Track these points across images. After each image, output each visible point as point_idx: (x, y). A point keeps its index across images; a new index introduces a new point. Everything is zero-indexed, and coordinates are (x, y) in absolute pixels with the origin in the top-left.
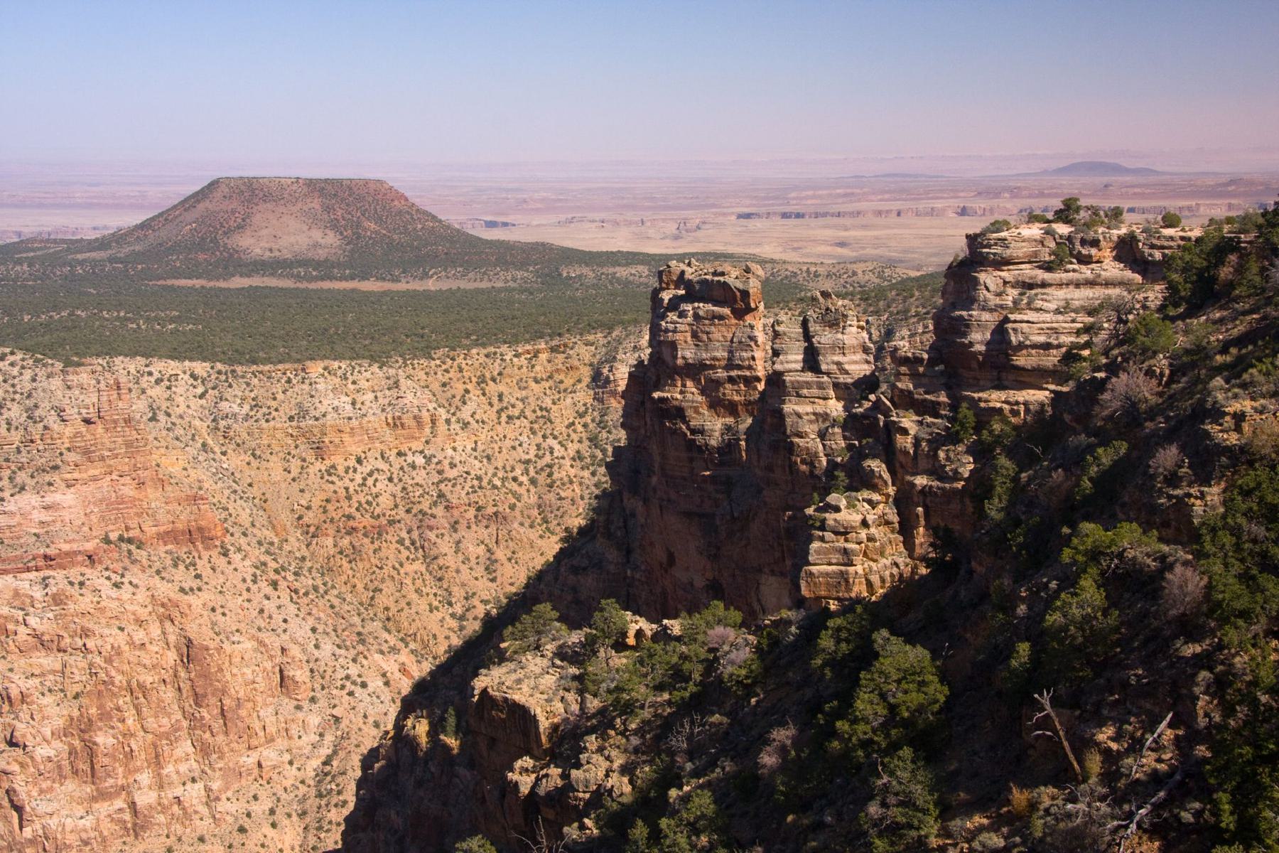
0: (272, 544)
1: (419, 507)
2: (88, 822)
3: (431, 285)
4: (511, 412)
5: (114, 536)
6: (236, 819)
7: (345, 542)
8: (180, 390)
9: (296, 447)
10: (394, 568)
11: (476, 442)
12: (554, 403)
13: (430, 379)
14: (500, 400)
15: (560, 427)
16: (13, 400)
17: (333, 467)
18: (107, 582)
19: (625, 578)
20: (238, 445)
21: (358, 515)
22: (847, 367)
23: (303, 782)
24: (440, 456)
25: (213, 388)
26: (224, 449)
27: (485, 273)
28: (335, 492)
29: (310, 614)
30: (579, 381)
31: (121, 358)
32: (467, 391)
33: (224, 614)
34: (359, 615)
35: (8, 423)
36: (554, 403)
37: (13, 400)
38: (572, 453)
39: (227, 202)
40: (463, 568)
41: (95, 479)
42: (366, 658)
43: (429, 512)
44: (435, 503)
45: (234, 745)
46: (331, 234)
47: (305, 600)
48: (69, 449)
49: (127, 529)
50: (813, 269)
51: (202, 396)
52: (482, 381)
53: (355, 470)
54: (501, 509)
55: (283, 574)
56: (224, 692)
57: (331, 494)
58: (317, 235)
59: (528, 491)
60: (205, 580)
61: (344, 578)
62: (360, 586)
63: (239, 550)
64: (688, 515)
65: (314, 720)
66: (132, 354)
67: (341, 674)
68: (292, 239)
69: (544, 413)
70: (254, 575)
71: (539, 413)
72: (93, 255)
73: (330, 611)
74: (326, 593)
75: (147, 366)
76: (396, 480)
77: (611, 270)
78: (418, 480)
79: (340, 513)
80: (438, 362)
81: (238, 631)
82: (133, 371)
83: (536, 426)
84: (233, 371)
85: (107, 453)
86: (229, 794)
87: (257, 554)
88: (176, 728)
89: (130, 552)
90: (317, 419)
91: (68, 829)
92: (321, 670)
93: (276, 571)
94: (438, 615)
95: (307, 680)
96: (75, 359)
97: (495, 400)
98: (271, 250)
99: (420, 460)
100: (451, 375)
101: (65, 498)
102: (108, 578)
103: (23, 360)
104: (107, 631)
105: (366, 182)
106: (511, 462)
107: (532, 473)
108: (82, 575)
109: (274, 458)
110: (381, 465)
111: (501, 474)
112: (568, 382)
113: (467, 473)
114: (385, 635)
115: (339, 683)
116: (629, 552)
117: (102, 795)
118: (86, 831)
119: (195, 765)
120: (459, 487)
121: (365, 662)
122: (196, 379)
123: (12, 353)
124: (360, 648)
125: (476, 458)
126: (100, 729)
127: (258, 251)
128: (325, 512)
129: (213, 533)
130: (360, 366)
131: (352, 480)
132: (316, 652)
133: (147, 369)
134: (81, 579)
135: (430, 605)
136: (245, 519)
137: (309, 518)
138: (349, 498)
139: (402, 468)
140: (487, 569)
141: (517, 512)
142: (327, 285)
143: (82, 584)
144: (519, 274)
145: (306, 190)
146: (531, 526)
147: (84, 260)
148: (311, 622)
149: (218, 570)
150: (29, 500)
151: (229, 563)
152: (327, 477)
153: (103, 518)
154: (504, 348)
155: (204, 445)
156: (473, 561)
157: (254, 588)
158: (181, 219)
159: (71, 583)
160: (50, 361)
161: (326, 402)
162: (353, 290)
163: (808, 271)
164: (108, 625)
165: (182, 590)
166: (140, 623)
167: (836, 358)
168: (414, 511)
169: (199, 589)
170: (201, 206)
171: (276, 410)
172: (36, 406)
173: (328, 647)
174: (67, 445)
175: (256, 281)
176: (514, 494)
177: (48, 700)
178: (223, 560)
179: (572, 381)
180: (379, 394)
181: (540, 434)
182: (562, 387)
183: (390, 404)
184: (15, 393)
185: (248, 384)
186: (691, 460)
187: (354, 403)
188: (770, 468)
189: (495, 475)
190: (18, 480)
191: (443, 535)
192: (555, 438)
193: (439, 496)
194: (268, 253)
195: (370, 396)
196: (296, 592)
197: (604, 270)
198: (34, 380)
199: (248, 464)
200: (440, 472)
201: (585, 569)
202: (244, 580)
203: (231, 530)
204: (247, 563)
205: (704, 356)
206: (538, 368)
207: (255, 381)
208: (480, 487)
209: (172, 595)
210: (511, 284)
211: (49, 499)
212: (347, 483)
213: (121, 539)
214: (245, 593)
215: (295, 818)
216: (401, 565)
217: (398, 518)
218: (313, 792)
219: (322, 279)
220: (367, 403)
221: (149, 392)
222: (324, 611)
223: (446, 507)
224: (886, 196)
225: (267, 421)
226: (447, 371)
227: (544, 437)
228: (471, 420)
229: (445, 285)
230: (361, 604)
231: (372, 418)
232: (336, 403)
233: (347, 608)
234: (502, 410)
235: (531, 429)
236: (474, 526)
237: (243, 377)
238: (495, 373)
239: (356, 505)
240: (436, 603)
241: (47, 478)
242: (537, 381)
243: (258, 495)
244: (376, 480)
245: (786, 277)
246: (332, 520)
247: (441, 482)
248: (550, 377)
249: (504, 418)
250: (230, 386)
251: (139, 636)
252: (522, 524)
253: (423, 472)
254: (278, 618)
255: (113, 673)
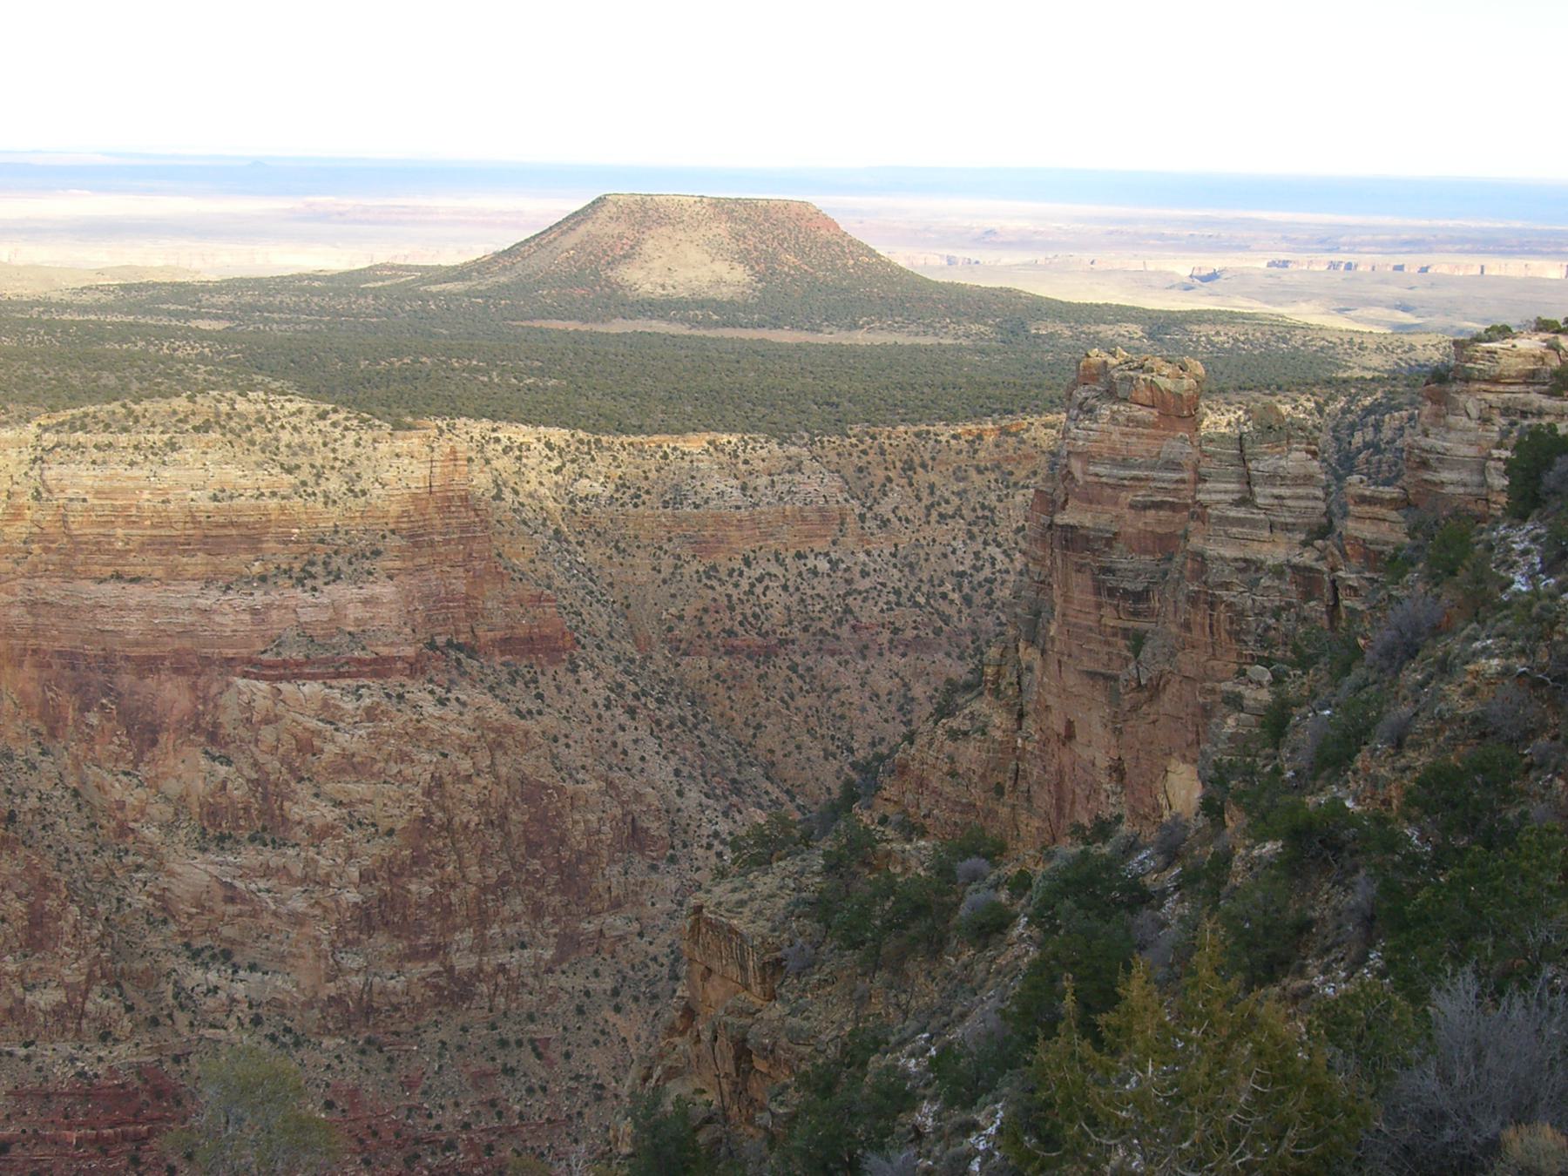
0: (632, 661)
1: (820, 625)
2: (398, 984)
3: (861, 338)
4: (944, 508)
5: (441, 640)
6: (572, 997)
7: (721, 664)
8: (531, 462)
9: (670, 540)
10: (782, 700)
11: (896, 546)
12: (1000, 500)
13: (843, 461)
14: (932, 493)
15: (1005, 533)
16: (333, 468)
17: (714, 568)
18: (430, 697)
19: (1015, 749)
20: (599, 534)
21: (740, 630)
22: (1289, 502)
23: (655, 959)
24: (849, 562)
25: (573, 461)
26: (581, 538)
27: (929, 325)
28: (715, 600)
29: (673, 752)
30: (1035, 473)
31: (464, 419)
32: (890, 480)
33: (568, 746)
34: (735, 756)
35: (326, 497)
36: (1000, 500)
37: (333, 468)
38: (1018, 565)
39: (613, 225)
40: (870, 705)
41: (420, 569)
42: (740, 812)
43: (831, 631)
44: (840, 622)
45: (573, 907)
46: (740, 268)
47: (667, 735)
48: (393, 532)
49: (457, 632)
50: (1357, 340)
51: (558, 471)
52: (909, 466)
53: (741, 574)
54: (922, 634)
55: (643, 699)
56: (562, 841)
57: (708, 602)
58: (721, 268)
59: (960, 612)
60: (548, 701)
61: (718, 709)
62: (739, 721)
63: (592, 666)
64: (1092, 675)
65: (671, 883)
66: (478, 415)
67: (707, 829)
68: (691, 275)
69: (987, 513)
70: (608, 698)
71: (980, 513)
72: (450, 286)
73: (698, 750)
74: (695, 726)
75: (494, 430)
76: (791, 590)
77: (1093, 329)
78: (820, 590)
79: (719, 626)
80: (854, 440)
81: (583, 767)
82: (477, 437)
83: (975, 529)
84: (599, 441)
85: (437, 538)
86: (565, 966)
87: (612, 671)
88: (503, 881)
89: (458, 660)
90: (697, 506)
91: (376, 989)
92: (683, 822)
93: (636, 696)
94: (836, 764)
95: (665, 834)
96: (409, 419)
97: (925, 494)
98: (663, 287)
99: (823, 566)
100: (869, 458)
101: (385, 590)
102: (432, 692)
103: (347, 419)
104: (426, 757)
105: (787, 204)
106: (940, 574)
107: (966, 590)
108: (403, 686)
109: (641, 553)
110: (774, 569)
111: (925, 589)
112: (1020, 474)
113: (883, 585)
114: (768, 785)
115: (704, 842)
116: (1021, 716)
117: (414, 955)
118: (395, 994)
119: (526, 929)
120: (871, 602)
121: (738, 817)
122: (552, 450)
123: (335, 411)
124: (734, 799)
125: (895, 566)
126: (416, 875)
127: (648, 287)
128: (701, 624)
129: (560, 643)
130: (755, 440)
131: (736, 585)
132: (678, 800)
133: (494, 435)
134: (400, 690)
135: (825, 750)
136: (601, 625)
137: (681, 631)
138: (732, 608)
139: (800, 574)
140: (901, 709)
141: (943, 639)
142: (728, 333)
143: (400, 697)
144: (975, 328)
145: (711, 211)
146: (961, 658)
147: (439, 293)
148: (674, 761)
149: (565, 690)
150: (343, 592)
151: (578, 682)
152: (705, 580)
153: (429, 619)
154: (939, 427)
155: (557, 532)
156: (884, 698)
157: (607, 715)
158: (556, 244)
159: (388, 696)
160: (377, 422)
161: (710, 484)
162: (761, 341)
163: (1351, 342)
164: (429, 750)
165: (519, 712)
166: (466, 749)
167: (1276, 491)
168: (812, 630)
169: (540, 713)
170: (582, 230)
171: (648, 492)
172: (358, 475)
173: (693, 795)
174: (392, 526)
175: (642, 325)
176: (941, 615)
177: (356, 834)
178: (571, 678)
179: (1024, 473)
180: (776, 478)
181: (980, 540)
182: (1012, 479)
183: (789, 492)
184: (336, 459)
185: (615, 458)
186: (1099, 606)
187: (744, 488)
188: (1187, 626)
189: (918, 589)
190: (333, 567)
191: (847, 662)
192: (999, 545)
193: (845, 612)
194: (659, 290)
195: (765, 480)
196: (658, 723)
197: (1085, 328)
198: (357, 445)
199: (610, 558)
200: (849, 582)
201: (966, 734)
202: (595, 705)
203: (583, 640)
204: (600, 683)
205: (1122, 473)
206: (982, 454)
207: (623, 455)
208: (898, 604)
209: (506, 717)
210: (965, 342)
211: (368, 591)
212: (731, 590)
213: (449, 644)
214: (594, 720)
215: (644, 1002)
216: (792, 698)
217: (791, 636)
218: (665, 971)
219: (724, 325)
220: (762, 489)
221: (495, 463)
222: (691, 750)
223: (853, 627)
224: (1467, 247)
225: (636, 506)
226: (864, 452)
227: (986, 543)
228: (891, 516)
229: (879, 338)
230: (740, 744)
231: (765, 509)
232: (721, 487)
233: (720, 747)
234: (932, 505)
235: (969, 531)
236: (887, 654)
237: (609, 449)
238: (927, 457)
239: (739, 618)
240: (832, 748)
241: (367, 565)
242: (980, 472)
243: (620, 599)
244: (767, 588)
245: (1322, 348)
246: (709, 636)
247: (848, 594)
248: (998, 466)
249: (934, 516)
250: (593, 460)
251: (465, 765)
252: (948, 655)
253: (827, 580)
254: (634, 756)
255: (433, 809)
